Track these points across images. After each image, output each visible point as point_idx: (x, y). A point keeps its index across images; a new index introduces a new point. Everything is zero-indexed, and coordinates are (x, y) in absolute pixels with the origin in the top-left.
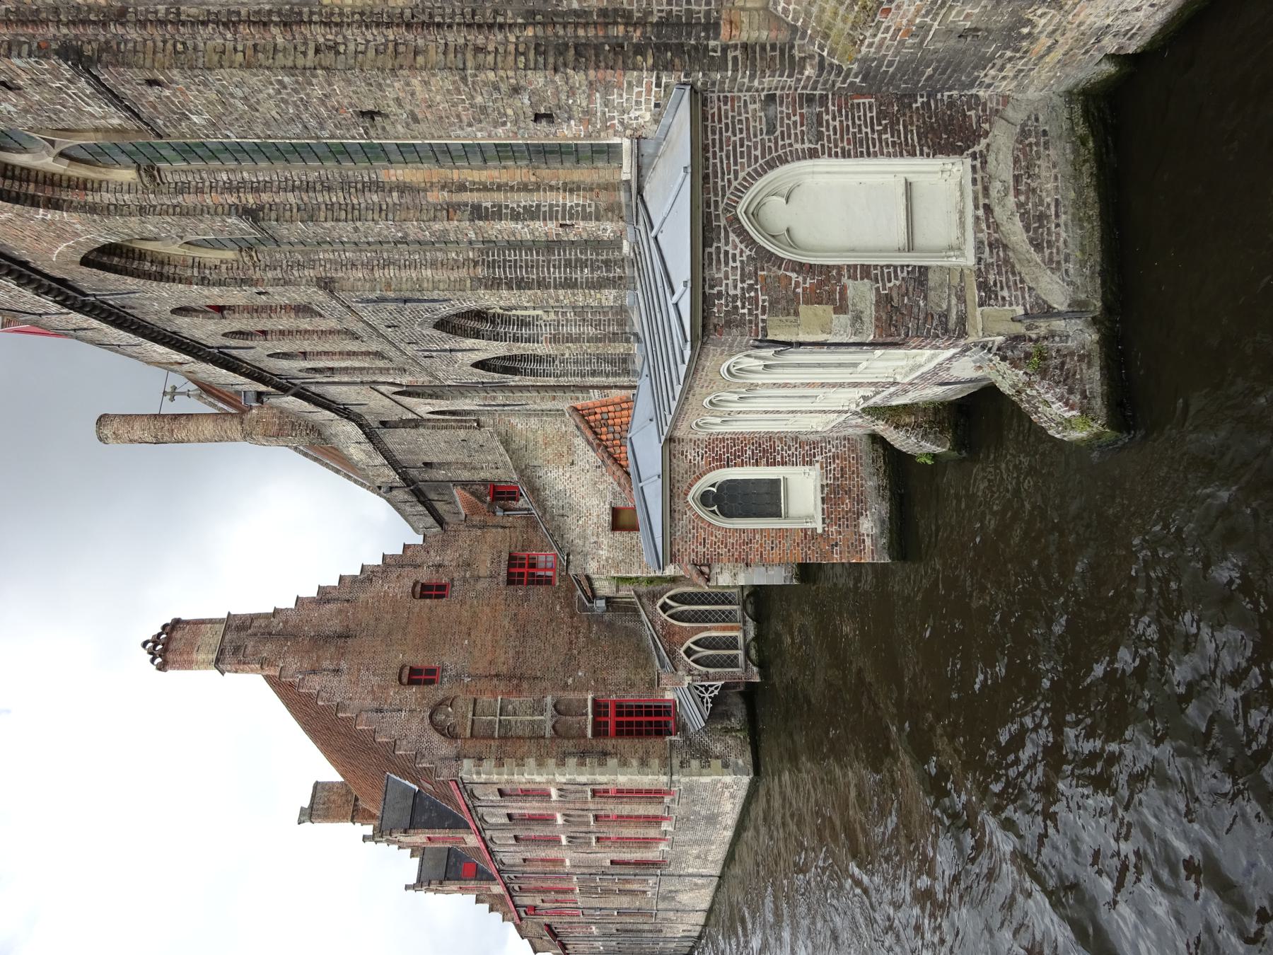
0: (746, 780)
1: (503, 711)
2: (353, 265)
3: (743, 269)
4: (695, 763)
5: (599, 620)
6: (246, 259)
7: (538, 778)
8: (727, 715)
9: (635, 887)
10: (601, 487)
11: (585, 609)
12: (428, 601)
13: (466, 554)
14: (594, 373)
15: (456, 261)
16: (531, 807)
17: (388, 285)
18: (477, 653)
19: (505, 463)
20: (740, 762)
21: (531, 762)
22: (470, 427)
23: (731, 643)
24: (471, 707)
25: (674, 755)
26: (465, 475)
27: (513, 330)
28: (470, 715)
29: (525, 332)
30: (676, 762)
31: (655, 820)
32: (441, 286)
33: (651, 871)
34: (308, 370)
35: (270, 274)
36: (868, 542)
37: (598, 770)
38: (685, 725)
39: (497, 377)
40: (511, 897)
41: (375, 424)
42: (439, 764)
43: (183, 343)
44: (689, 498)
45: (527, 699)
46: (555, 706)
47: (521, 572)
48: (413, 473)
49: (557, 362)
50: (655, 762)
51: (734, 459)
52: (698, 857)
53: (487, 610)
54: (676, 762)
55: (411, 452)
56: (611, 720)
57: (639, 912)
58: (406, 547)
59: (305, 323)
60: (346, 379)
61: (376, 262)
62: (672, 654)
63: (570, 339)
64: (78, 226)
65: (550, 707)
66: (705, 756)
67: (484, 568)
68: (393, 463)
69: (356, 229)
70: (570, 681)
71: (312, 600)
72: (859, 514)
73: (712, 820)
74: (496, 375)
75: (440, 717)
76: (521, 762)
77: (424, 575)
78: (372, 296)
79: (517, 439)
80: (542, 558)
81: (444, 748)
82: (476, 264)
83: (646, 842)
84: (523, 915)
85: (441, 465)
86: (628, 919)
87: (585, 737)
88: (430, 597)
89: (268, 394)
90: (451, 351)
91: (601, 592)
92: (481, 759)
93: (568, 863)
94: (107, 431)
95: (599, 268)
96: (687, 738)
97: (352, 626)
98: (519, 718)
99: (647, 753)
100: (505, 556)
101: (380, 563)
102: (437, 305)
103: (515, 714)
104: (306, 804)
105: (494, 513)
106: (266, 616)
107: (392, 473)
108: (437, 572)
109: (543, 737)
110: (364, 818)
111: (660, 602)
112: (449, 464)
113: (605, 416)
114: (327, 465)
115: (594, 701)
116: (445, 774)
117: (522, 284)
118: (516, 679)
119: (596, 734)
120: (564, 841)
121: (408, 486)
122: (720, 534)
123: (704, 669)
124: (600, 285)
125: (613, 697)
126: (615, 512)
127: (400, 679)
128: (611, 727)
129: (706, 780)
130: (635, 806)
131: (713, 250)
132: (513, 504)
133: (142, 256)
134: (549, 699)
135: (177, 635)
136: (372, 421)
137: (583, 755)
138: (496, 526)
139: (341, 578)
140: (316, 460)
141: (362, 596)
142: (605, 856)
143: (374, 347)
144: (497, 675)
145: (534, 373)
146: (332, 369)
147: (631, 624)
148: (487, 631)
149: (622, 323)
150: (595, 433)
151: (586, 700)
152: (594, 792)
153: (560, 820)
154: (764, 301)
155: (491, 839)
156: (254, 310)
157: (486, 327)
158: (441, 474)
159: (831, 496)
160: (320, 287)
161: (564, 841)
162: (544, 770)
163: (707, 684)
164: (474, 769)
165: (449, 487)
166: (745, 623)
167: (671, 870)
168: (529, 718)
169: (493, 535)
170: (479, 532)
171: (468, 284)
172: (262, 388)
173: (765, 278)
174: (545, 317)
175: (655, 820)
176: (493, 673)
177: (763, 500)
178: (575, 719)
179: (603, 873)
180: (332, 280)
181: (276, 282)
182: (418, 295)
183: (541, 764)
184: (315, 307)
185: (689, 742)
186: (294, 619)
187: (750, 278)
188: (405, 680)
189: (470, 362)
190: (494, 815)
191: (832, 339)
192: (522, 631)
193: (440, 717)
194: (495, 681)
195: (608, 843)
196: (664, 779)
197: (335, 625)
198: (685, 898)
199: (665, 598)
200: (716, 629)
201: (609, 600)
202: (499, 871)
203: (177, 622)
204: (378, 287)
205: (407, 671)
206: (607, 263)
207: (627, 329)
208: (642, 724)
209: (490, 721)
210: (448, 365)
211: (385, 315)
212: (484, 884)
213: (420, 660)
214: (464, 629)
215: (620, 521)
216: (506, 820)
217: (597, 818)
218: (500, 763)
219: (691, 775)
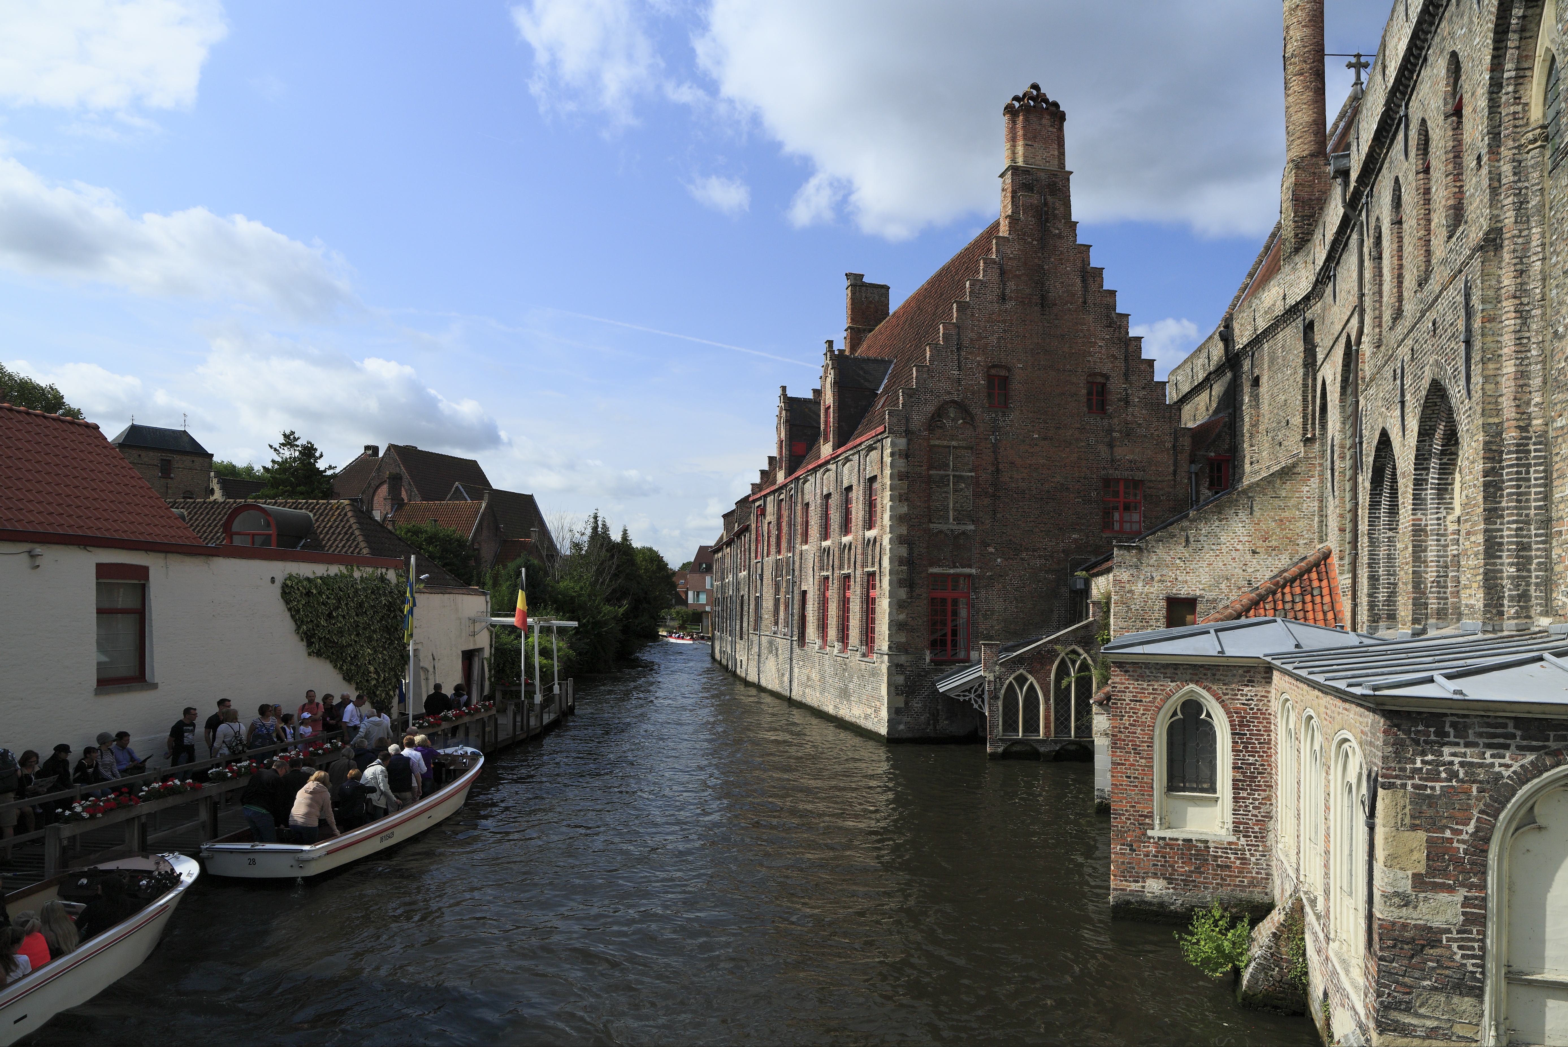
1: (959, 479)
2: (1522, 272)
3: (1481, 765)
6: (1530, 136)
12: (1084, 391)
15: (1528, 403)
17: (1491, 320)
19: (1257, 472)
21: (904, 509)
22: (1305, 429)
27: (1433, 477)
28: (954, 443)
29: (1430, 493)
32: (1490, 387)
34: (1378, 228)
35: (1506, 169)
39: (1369, 459)
41: (1309, 315)
43: (1412, 72)
46: (964, 533)
49: (1390, 534)
50: (902, 638)
55: (1272, 360)
57: (758, 618)
58: (1151, 363)
59: (1439, 218)
60: (1368, 275)
61: (1525, 300)
63: (1418, 550)
65: (963, 528)
68: (1257, 341)
70: (991, 550)
71: (1086, 261)
74: (1371, 459)
78: (1475, 301)
79: (1288, 485)
82: (1523, 429)
83: (823, 627)
85: (1256, 398)
86: (752, 606)
87: (931, 565)
88: (1089, 393)
89: (1346, 184)
90: (1403, 403)
101: (1130, 335)
102: (1462, 382)
103: (955, 491)
105: (1192, 462)
108: (1120, 400)
109: (930, 521)
113: (1316, 592)
117: (1492, 488)
119: (932, 574)
121: (1228, 360)
127: (994, 366)
130: (858, 616)
131: (1511, 729)
138: (1175, 464)
141: (1090, 318)
142: (810, 585)
143: (1410, 308)
144: (998, 471)
145: (1374, 505)
147: (1055, 616)
151: (970, 567)
152: (873, 574)
154: (1433, 788)
156: (1457, 154)
160: (1487, 233)
167: (797, 650)
168: (951, 505)
171: (1497, 420)
172: (1354, 175)
173: (1468, 793)
174: (1450, 518)
176: (1001, 466)
179: (794, 582)
180: (1498, 248)
181: (1495, 178)
182: (1476, 356)
184: (1461, 229)
187: (1466, 773)
188: (993, 371)
189: (1388, 426)
191: (1378, 866)
194: (991, 469)
196: (885, 647)
204: (1489, 306)
205: (1003, 373)
207: (1432, 621)
209: (948, 465)
210: (1384, 399)
211: (1449, 318)
213: (1017, 385)
217: (847, 577)
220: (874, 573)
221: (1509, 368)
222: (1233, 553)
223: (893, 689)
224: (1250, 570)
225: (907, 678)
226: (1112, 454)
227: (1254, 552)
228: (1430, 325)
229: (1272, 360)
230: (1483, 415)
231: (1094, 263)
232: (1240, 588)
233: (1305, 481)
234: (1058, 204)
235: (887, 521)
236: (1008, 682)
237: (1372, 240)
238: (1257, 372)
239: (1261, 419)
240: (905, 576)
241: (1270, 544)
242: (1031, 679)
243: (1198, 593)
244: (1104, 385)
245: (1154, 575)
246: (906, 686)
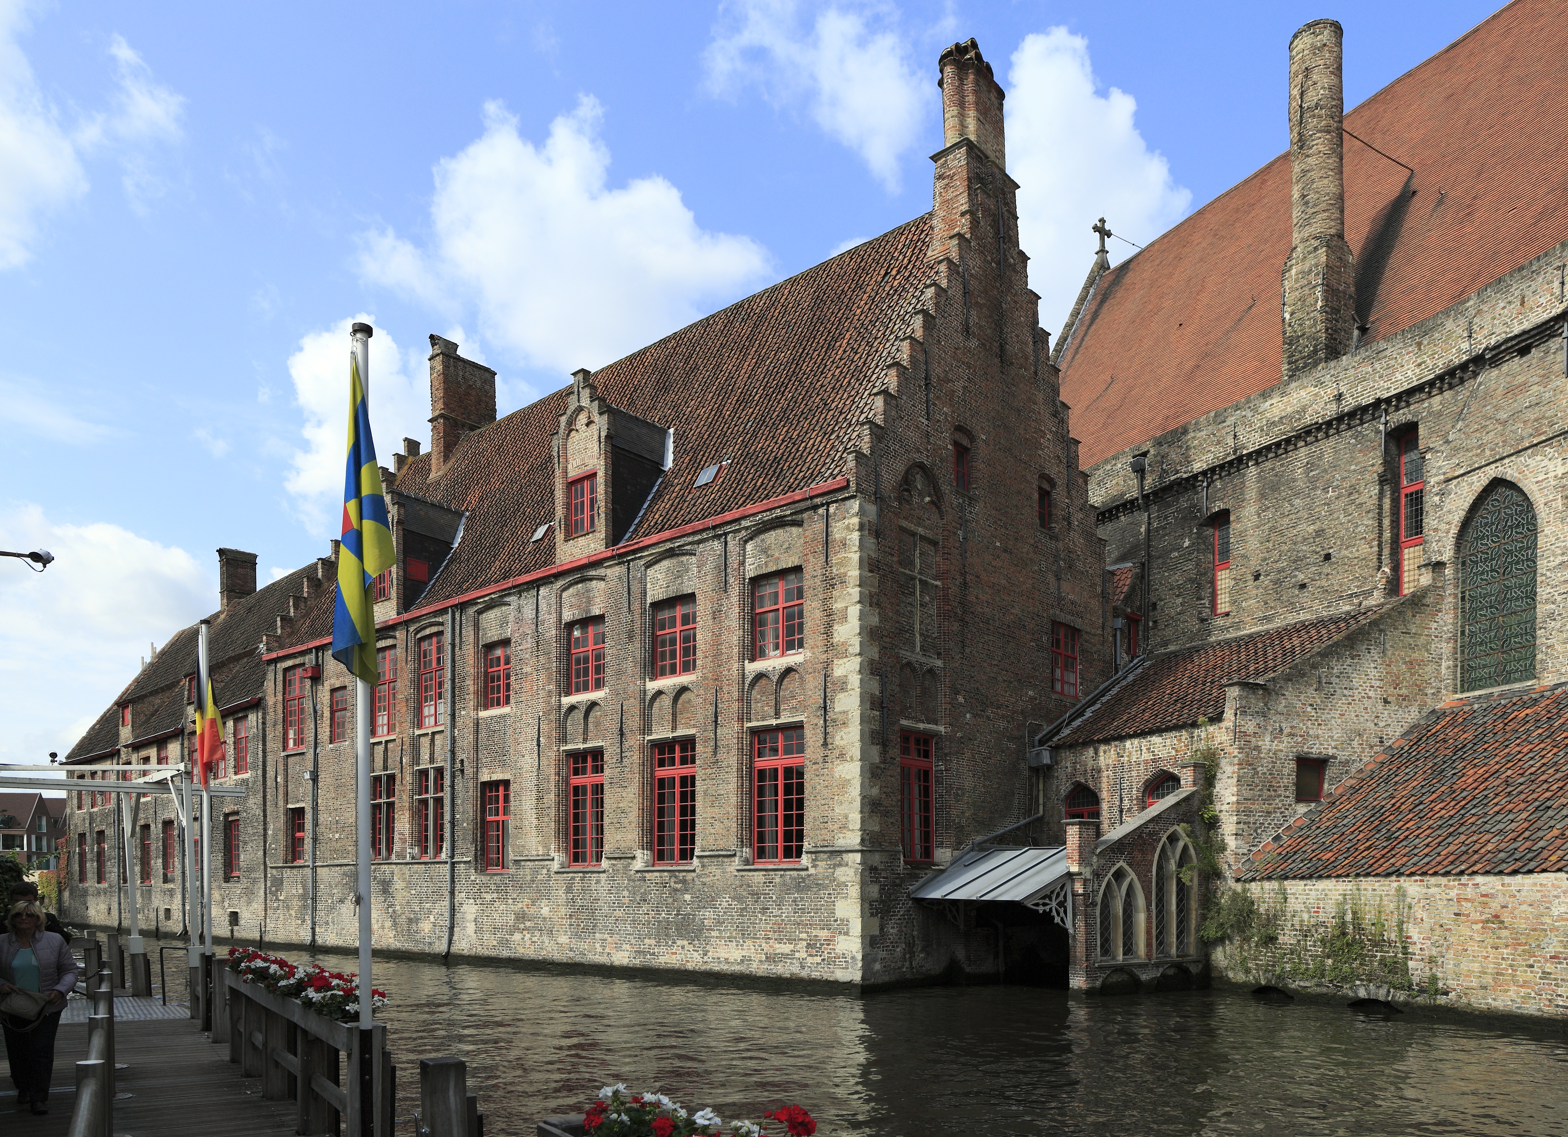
54: (876, 859)
91: (1067, 760)
219: (863, 884)
223: (867, 905)
224: (1382, 724)
225: (882, 889)
226: (1059, 589)
227: (1386, 701)
232: (1371, 747)
235: (849, 631)
236: (1106, 879)
241: (1401, 692)
242: (1132, 875)
243: (1331, 752)
244: (1048, 493)
245: (1284, 725)
246: (881, 901)
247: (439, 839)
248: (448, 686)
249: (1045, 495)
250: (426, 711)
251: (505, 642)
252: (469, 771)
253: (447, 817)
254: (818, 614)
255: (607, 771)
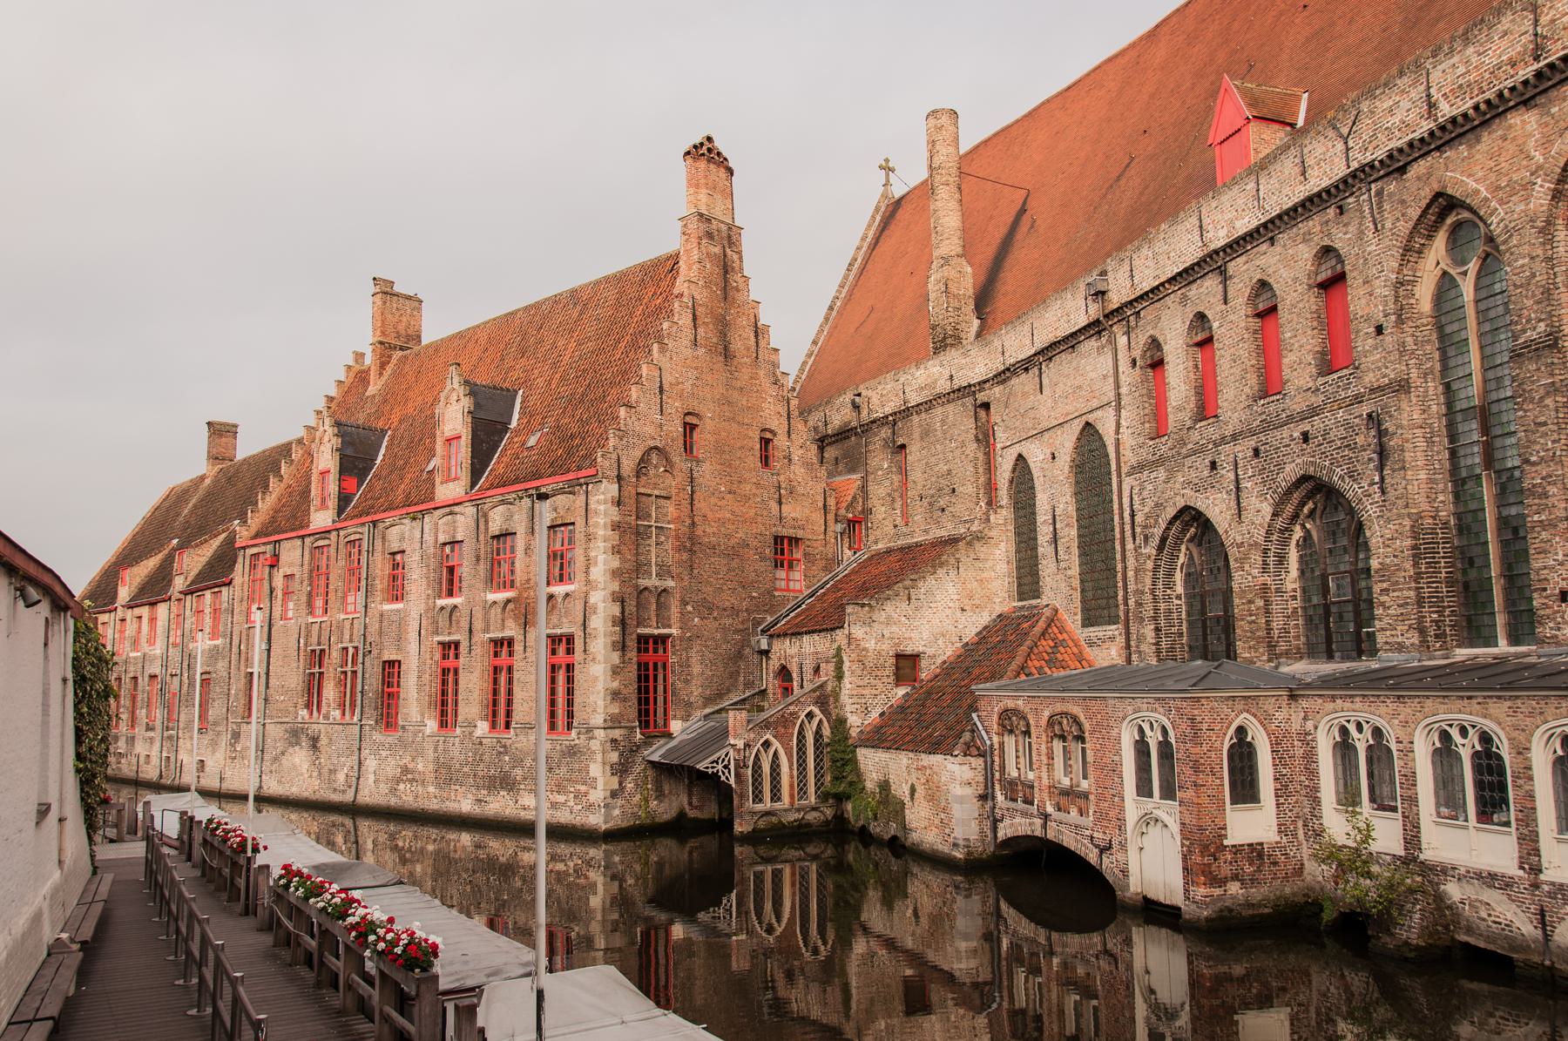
0: (596, 820)
4: (614, 757)
5: (745, 643)
7: (599, 572)
8: (660, 795)
9: (330, 692)
10: (940, 642)
11: (757, 623)
13: (800, 490)
14: (1157, 630)
16: (530, 561)
18: (713, 500)
20: (617, 812)
21: (616, 563)
23: (776, 796)
24: (663, 493)
25: (622, 731)
26: (878, 491)
28: (656, 492)
29: (1271, 560)
30: (617, 734)
31: (500, 710)
33: (369, 711)
34: (1155, 344)
36: (1218, 892)
37: (609, 641)
38: (651, 745)
40: (303, 537)
42: (614, 456)
44: (1245, 715)
45: (671, 557)
47: (783, 548)
48: (885, 432)
51: (1279, 757)
52: (405, 770)
53: (752, 513)
54: (617, 734)
55: (926, 433)
56: (650, 657)
62: (766, 725)
63: (1267, 603)
64: (1522, 207)
66: (621, 770)
67: (791, 510)
68: (905, 412)
69: (1545, 424)
70: (689, 608)
72: (1242, 882)
73: (505, 783)
74: (1158, 532)
75: (654, 458)
76: (616, 550)
77: (781, 441)
80: (796, 575)
81: (628, 466)
82: (1434, 518)
84: (255, 550)
92: (619, 503)
93: (387, 607)
94: (944, 120)
95: (1439, 628)
96: (638, 747)
97: (735, 361)
98: (653, 549)
99: (625, 700)
100: (800, 534)
104: (396, 289)
105: (836, 521)
106: (741, 269)
107: (888, 410)
110: (382, 356)
111: (816, 711)
112: (903, 472)
114: (821, 331)
115: (669, 636)
116: (604, 463)
118: (690, 544)
120: (441, 602)
122: (1217, 744)
123: (751, 763)
124: (1422, 631)
125: (672, 659)
126: (915, 658)
128: (645, 657)
129: (595, 769)
132: (846, 540)
133: (1430, 237)
134: (670, 583)
135: (722, 173)
136: (995, 393)
137: (622, 622)
139: (777, 350)
140: (827, 319)
144: (693, 524)
145: (1156, 569)
146: (1157, 364)
148: (733, 513)
149: (1287, 654)
150: (1043, 634)
153: (491, 597)
155: (451, 513)
157: (1280, 523)
158: (880, 460)
159: (1256, 852)
161: (441, 602)
162: (608, 576)
163: (732, 767)
164: (609, 496)
165: (852, 470)
166: (798, 810)
169: (818, 518)
170: (821, 504)
175: (500, 710)
177: (1245, 789)
178: (653, 614)
183: (615, 573)
185: (635, 749)
186: (740, 297)
188: (689, 419)
190: (509, 518)
192: (734, 553)
193: (654, 458)
194: (688, 521)
195: (438, 656)
196: (598, 720)
197: (737, 345)
198: (299, 757)
199: (819, 715)
200: (792, 777)
201: (766, 653)
202: (374, 523)
203: (730, 171)
206: (1444, 635)
208: (647, 694)
212: (332, 503)
214: (734, 487)
215: (906, 664)
216: (495, 526)
217: (502, 645)
218: (616, 527)
220: (570, 639)
221: (1423, 475)
222: (948, 612)
228: (1296, 434)
229: (926, 433)
230: (1407, 506)
231: (762, 321)
233: (997, 545)
234: (735, 257)
237: (1137, 353)
238: (900, 441)
239: (910, 485)
240: (617, 638)
247: (353, 705)
248: (363, 583)
249: (766, 442)
250: (351, 599)
251: (403, 552)
252: (375, 652)
253: (359, 688)
254: (582, 558)
255: (461, 660)
